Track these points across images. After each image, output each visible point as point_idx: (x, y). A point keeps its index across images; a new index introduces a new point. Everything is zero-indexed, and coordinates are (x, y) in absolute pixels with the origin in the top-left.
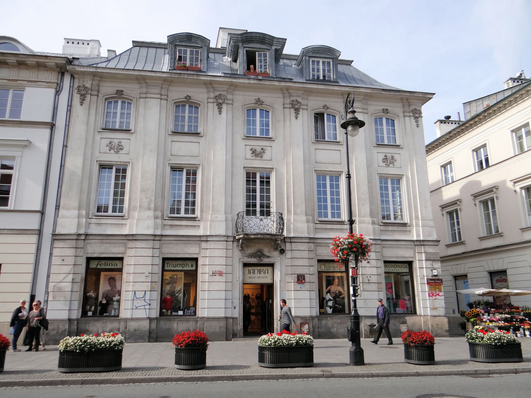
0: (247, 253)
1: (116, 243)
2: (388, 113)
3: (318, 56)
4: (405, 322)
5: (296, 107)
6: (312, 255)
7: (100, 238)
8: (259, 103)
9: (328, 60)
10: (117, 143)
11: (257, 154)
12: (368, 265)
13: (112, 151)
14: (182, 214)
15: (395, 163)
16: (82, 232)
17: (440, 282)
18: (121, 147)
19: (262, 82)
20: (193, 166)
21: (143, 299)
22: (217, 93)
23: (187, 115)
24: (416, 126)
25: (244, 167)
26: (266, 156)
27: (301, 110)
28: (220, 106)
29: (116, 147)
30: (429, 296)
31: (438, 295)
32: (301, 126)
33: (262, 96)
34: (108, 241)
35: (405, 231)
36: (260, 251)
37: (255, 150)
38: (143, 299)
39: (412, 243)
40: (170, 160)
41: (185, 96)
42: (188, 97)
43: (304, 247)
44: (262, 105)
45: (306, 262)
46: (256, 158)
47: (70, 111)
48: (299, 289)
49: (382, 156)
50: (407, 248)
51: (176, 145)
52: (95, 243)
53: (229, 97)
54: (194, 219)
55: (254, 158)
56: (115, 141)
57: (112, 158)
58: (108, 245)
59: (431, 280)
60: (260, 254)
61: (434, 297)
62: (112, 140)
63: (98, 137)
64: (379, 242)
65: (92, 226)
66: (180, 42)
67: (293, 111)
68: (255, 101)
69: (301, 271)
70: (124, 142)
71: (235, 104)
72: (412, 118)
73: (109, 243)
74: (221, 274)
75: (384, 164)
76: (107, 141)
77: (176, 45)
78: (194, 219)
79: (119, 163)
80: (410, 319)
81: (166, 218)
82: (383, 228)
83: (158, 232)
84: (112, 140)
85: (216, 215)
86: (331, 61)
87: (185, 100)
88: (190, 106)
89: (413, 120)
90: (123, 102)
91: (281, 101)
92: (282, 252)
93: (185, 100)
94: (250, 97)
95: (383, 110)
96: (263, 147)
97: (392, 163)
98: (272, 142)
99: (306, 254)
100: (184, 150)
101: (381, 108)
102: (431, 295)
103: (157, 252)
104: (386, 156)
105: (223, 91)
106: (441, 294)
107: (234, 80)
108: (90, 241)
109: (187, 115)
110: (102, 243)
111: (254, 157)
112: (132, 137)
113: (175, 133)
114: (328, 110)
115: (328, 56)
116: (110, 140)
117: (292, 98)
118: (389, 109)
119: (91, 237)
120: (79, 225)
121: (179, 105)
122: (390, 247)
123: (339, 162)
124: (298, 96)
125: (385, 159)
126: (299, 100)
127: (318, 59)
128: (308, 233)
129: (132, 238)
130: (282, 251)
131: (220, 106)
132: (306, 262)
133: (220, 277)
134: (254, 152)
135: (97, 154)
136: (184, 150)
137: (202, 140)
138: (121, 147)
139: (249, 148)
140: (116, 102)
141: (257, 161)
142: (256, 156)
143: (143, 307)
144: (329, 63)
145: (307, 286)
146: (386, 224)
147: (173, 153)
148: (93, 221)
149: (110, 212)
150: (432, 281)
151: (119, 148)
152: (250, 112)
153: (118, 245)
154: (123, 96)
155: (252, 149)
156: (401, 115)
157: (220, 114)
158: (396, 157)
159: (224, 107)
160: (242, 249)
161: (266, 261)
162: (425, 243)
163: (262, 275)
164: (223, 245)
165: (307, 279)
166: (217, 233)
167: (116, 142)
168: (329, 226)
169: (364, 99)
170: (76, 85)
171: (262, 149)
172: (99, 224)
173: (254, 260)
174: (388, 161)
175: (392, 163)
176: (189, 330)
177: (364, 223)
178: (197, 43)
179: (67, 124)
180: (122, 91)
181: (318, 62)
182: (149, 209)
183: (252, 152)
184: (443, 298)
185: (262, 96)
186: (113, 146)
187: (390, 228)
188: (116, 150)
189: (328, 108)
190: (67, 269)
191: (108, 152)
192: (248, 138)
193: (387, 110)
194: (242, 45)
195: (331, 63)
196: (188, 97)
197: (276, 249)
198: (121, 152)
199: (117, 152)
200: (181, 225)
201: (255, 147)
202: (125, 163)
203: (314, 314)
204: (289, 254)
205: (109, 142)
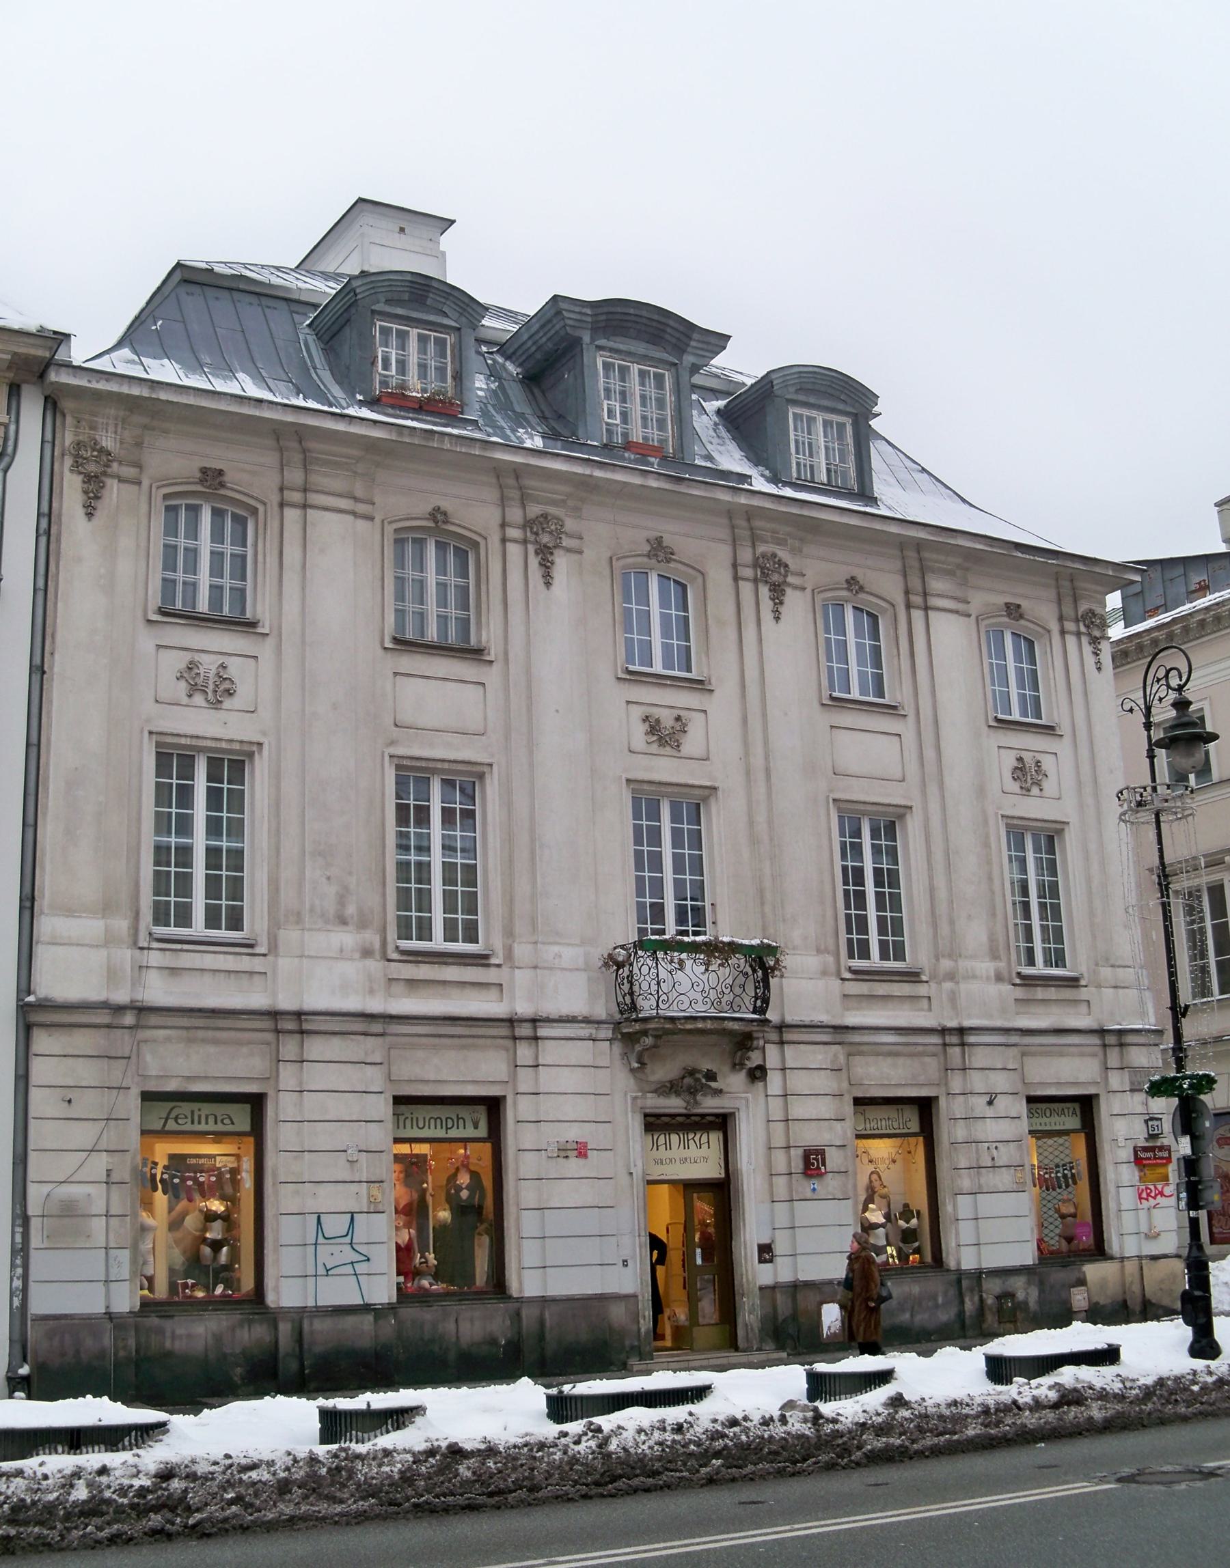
0: (653, 1078)
1: (240, 1043)
2: (1021, 617)
3: (812, 400)
4: (1082, 1282)
5: (775, 578)
7: (185, 1022)
8: (661, 555)
9: (841, 419)
10: (213, 672)
11: (664, 735)
12: (989, 1112)
13: (199, 699)
14: (438, 942)
15: (1045, 784)
17: (1166, 1155)
18: (226, 685)
19: (682, 488)
20: (469, 768)
21: (348, 1240)
22: (534, 510)
23: (432, 578)
24: (1094, 667)
25: (628, 781)
26: (692, 743)
27: (789, 591)
28: (545, 556)
29: (211, 687)
30: (1141, 1198)
31: (1161, 1194)
32: (788, 646)
33: (673, 531)
34: (210, 1034)
35: (1076, 1002)
37: (658, 721)
38: (348, 1240)
40: (392, 743)
41: (429, 508)
42: (438, 515)
43: (818, 1056)
44: (668, 561)
45: (824, 1108)
46: (662, 751)
47: (48, 533)
48: (809, 1195)
49: (1009, 760)
50: (1082, 1055)
51: (411, 687)
52: (168, 1039)
53: (570, 524)
54: (481, 960)
55: (654, 748)
56: (204, 659)
57: (200, 723)
58: (212, 1049)
59: (1145, 1149)
61: (1152, 1202)
62: (197, 657)
63: (146, 641)
64: (1014, 1039)
65: (153, 978)
66: (388, 302)
67: (764, 591)
68: (647, 548)
69: (811, 1136)
70: (236, 668)
71: (589, 554)
72: (1085, 640)
73: (216, 1042)
74: (582, 1151)
75: (1014, 787)
76: (177, 661)
77: (373, 312)
78: (481, 960)
79: (224, 745)
80: (1093, 1271)
81: (395, 956)
82: (1020, 993)
83: (375, 1005)
84: (197, 657)
85: (556, 949)
86: (848, 421)
87: (431, 524)
88: (441, 547)
89: (1087, 649)
90: (217, 513)
91: (725, 551)
92: (758, 1074)
93: (431, 524)
94: (635, 532)
95: (1008, 605)
96: (682, 713)
97: (1038, 783)
98: (707, 695)
99: (825, 1082)
100: (442, 708)
101: (1001, 600)
102: (1144, 1195)
103: (374, 1078)
104: (1020, 759)
105: (554, 503)
106: (1167, 1191)
107: (598, 473)
108: (148, 1034)
109: (432, 578)
110: (190, 1041)
111: (655, 746)
112: (265, 650)
113: (403, 644)
114: (862, 596)
115: (841, 406)
116: (188, 656)
117: (762, 548)
118: (1025, 604)
119: (154, 1019)
120: (112, 974)
121: (407, 541)
122: (1042, 1054)
123: (899, 776)
124: (781, 542)
125: (1020, 771)
126: (783, 554)
127: (813, 413)
129: (291, 1024)
130: (758, 1074)
131: (545, 556)
132: (824, 1108)
133: (581, 1161)
134: (653, 727)
136: (442, 708)
137: (492, 676)
138: (226, 685)
139: (637, 712)
140: (194, 510)
142: (662, 742)
143: (349, 1269)
144: (841, 427)
145: (831, 1184)
146: (1028, 981)
147: (406, 717)
149: (198, 927)
150: (1148, 1155)
151: (219, 691)
152: (629, 583)
153: (245, 1050)
154: (222, 492)
155: (646, 719)
156: (1054, 627)
157: (548, 584)
158: (1048, 763)
159: (561, 562)
160: (640, 1068)
161: (709, 1104)
163: (693, 1151)
164: (581, 1052)
165: (830, 1165)
166: (566, 1009)
167: (209, 665)
168: (881, 989)
169: (958, 566)
170: (69, 438)
171: (678, 719)
172: (173, 971)
173: (674, 1104)
174: (1027, 775)
175: (1038, 783)
176: (493, 1342)
177: (974, 977)
178: (445, 315)
179: (41, 583)
180: (220, 473)
181: (811, 420)
182: (343, 921)
183: (646, 727)
185: (673, 531)
186: (200, 681)
187: (1040, 993)
188: (210, 696)
189: (861, 588)
190: (83, 1135)
191: (185, 700)
192: (634, 677)
193: (1019, 606)
194: (593, 340)
195: (849, 430)
196: (438, 515)
197: (737, 1066)
198: (228, 703)
199: (216, 705)
200: (444, 983)
201: (657, 712)
202: (246, 748)
204: (774, 1082)
205: (183, 665)
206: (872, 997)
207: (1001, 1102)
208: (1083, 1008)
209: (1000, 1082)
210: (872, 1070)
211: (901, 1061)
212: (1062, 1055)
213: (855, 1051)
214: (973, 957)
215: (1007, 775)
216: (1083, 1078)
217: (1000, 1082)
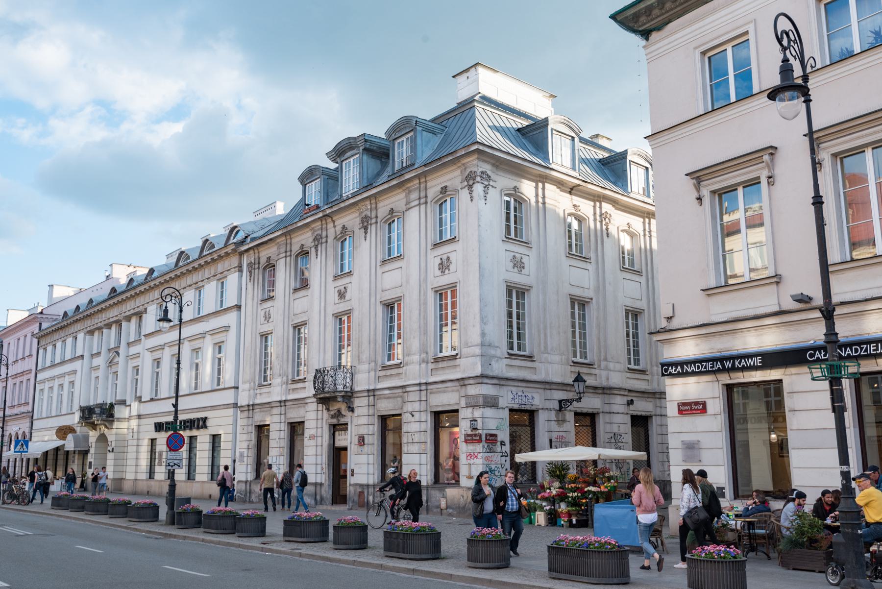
6: (371, 412)
12: (413, 419)
15: (451, 267)
16: (251, 403)
26: (348, 297)
35: (455, 366)
36: (339, 411)
39: (456, 384)
50: (453, 391)
53: (324, 234)
60: (339, 414)
65: (258, 396)
69: (363, 431)
75: (438, 273)
92: (352, 410)
128: (369, 384)
135: (259, 327)
139: (337, 289)
141: (342, 305)
145: (366, 449)
148: (258, 391)
160: (328, 410)
161: (342, 420)
162: (467, 382)
165: (366, 442)
184: (481, 461)
187: (441, 365)
203: (371, 482)
206: (386, 376)
207: (417, 415)
208: (458, 369)
209: (416, 406)
210: (383, 405)
211: (391, 400)
212: (445, 392)
213: (381, 397)
214: (414, 354)
215: (437, 267)
216: (452, 402)
217: (416, 406)
